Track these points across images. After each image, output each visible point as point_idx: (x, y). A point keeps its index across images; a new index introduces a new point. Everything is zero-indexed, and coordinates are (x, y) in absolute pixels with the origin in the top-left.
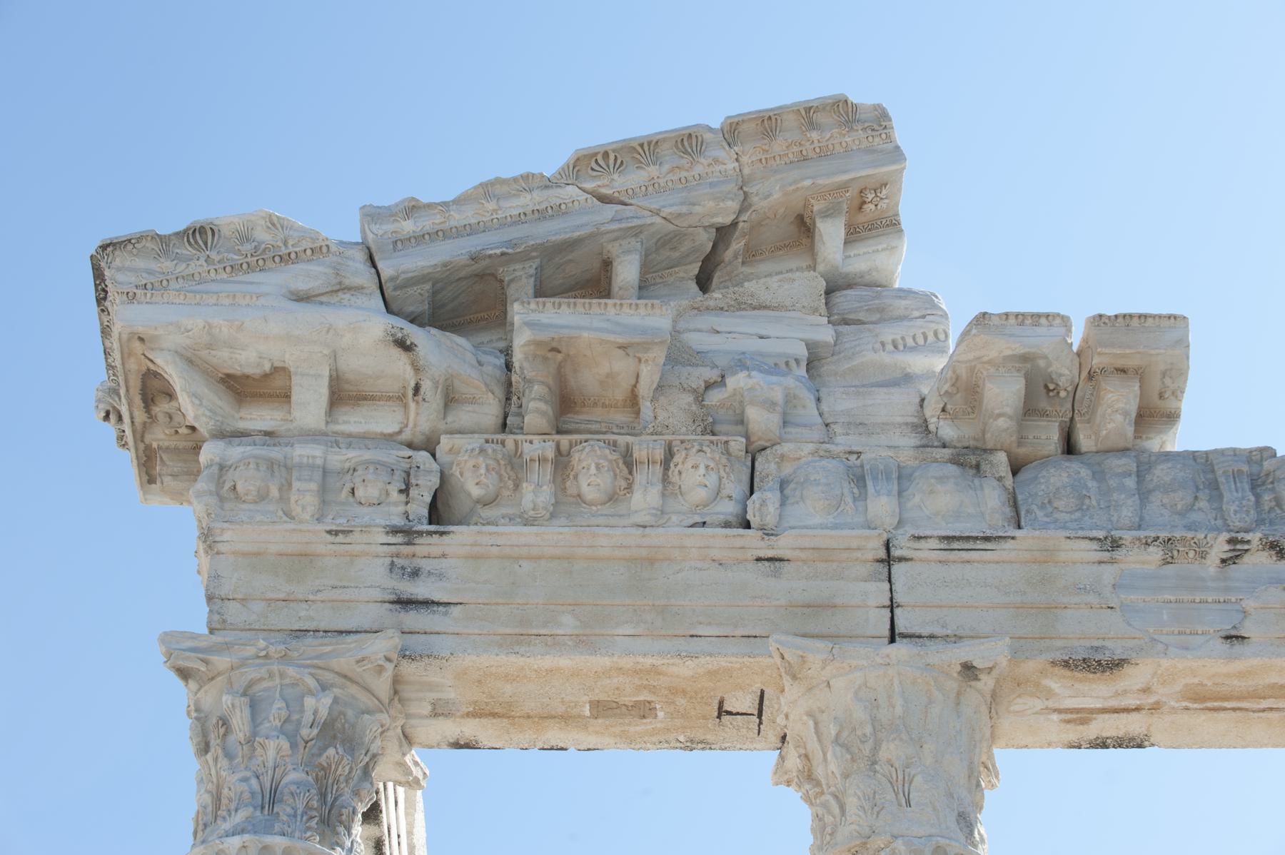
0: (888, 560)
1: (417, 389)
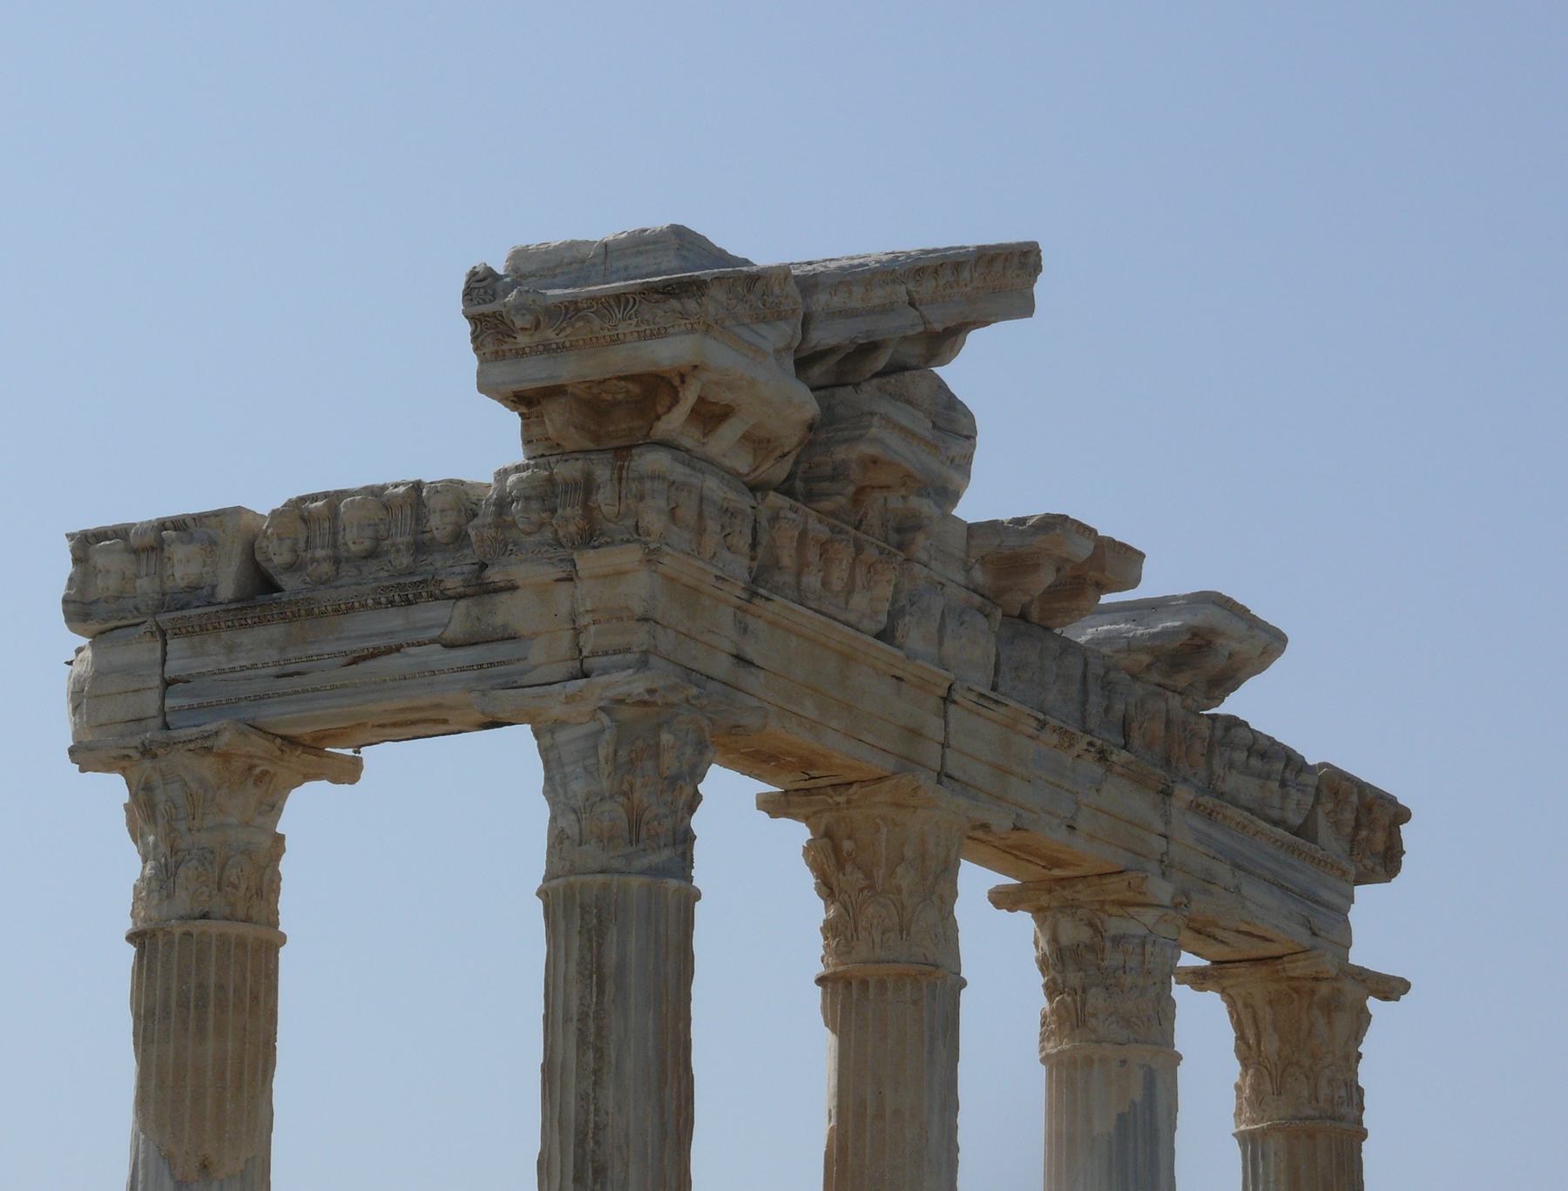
0: (947, 699)
1: (784, 455)
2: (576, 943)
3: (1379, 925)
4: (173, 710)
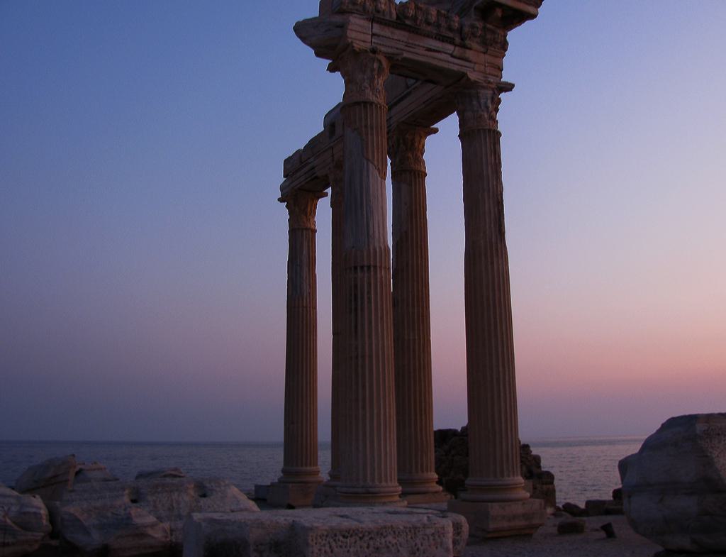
4: (374, 43)
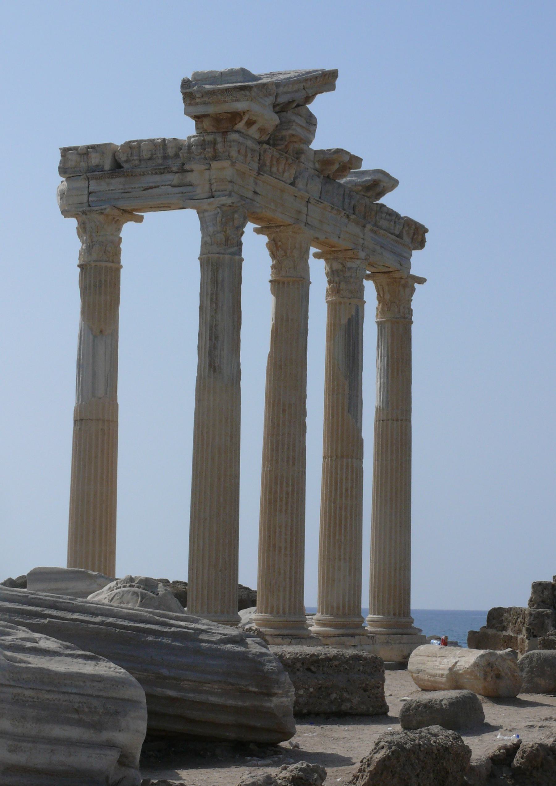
0: (308, 202)
2: (210, 273)
3: (419, 262)
4: (92, 201)
